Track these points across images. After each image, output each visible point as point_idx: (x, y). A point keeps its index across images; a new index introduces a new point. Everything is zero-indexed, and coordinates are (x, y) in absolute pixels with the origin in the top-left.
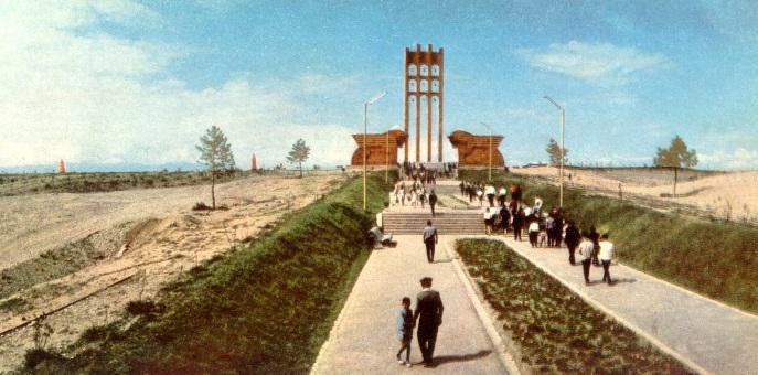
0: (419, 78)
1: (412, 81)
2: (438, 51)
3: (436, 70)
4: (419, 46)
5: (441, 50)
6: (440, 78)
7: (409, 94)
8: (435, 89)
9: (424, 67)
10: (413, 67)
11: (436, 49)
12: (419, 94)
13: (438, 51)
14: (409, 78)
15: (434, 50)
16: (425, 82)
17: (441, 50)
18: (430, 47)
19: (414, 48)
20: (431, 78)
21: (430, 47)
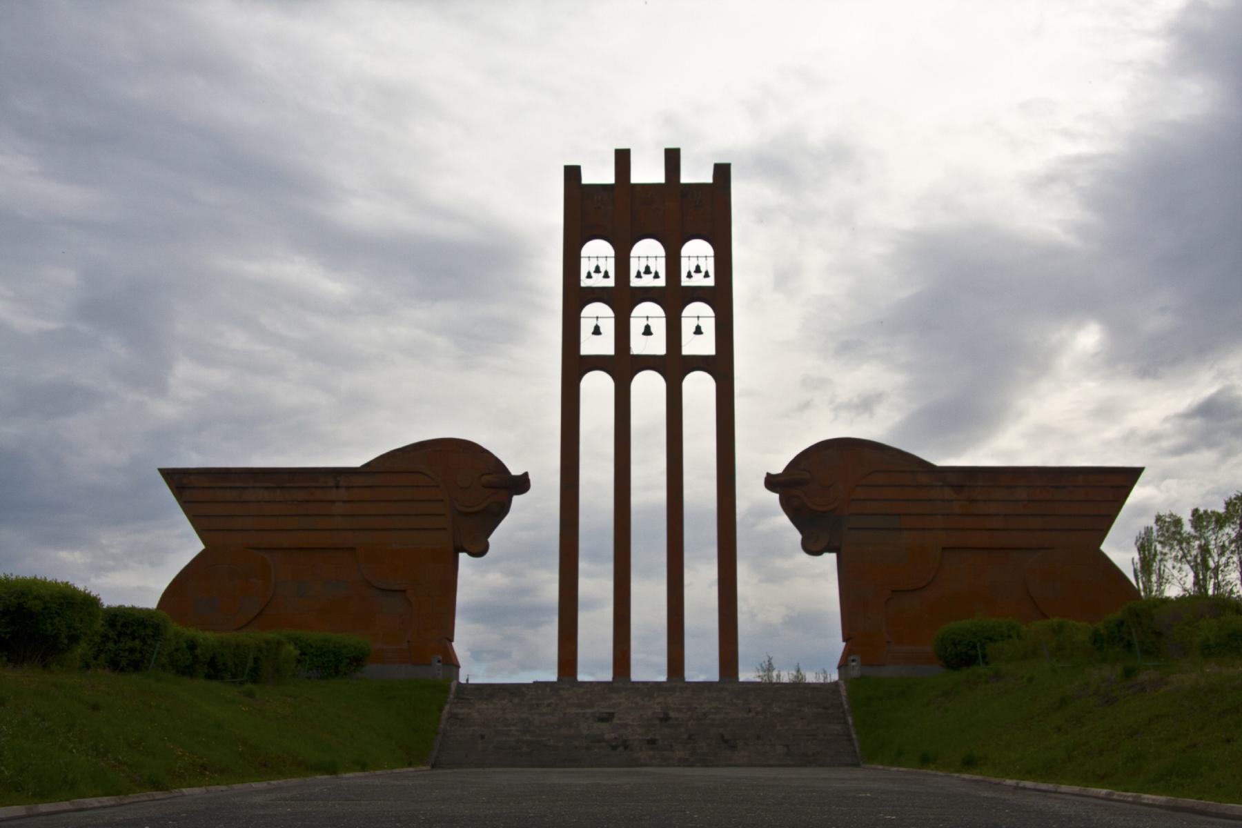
0: (623, 298)
1: (598, 314)
2: (707, 178)
3: (698, 253)
4: (623, 159)
5: (722, 172)
6: (720, 297)
7: (575, 366)
8: (700, 344)
9: (648, 254)
10: (598, 254)
11: (695, 173)
12: (623, 366)
13: (707, 178)
14: (576, 297)
15: (688, 176)
16: (648, 314)
17: (722, 172)
18: (672, 158)
19: (600, 173)
20: (674, 298)
21: (672, 158)
